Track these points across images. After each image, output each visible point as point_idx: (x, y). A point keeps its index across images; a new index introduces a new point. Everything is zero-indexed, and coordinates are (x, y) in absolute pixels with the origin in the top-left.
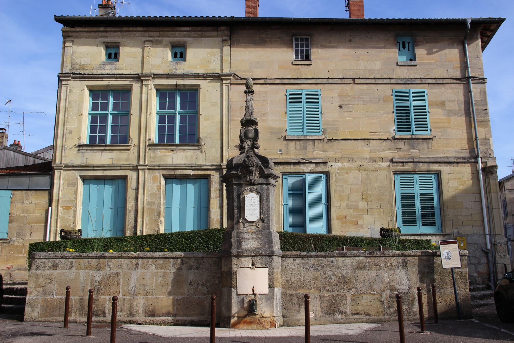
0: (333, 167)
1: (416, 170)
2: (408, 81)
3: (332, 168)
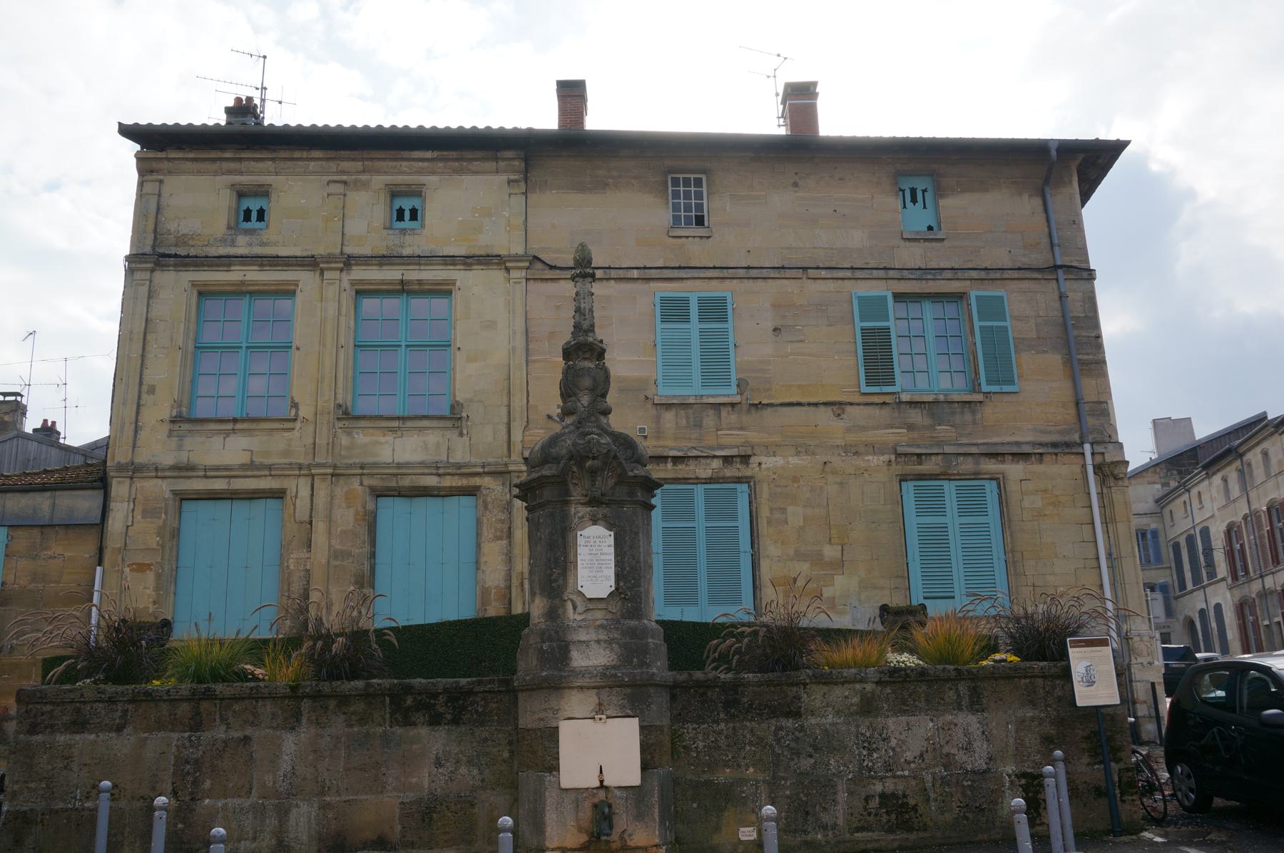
0: (763, 466)
1: (950, 472)
2: (926, 274)
3: (760, 469)
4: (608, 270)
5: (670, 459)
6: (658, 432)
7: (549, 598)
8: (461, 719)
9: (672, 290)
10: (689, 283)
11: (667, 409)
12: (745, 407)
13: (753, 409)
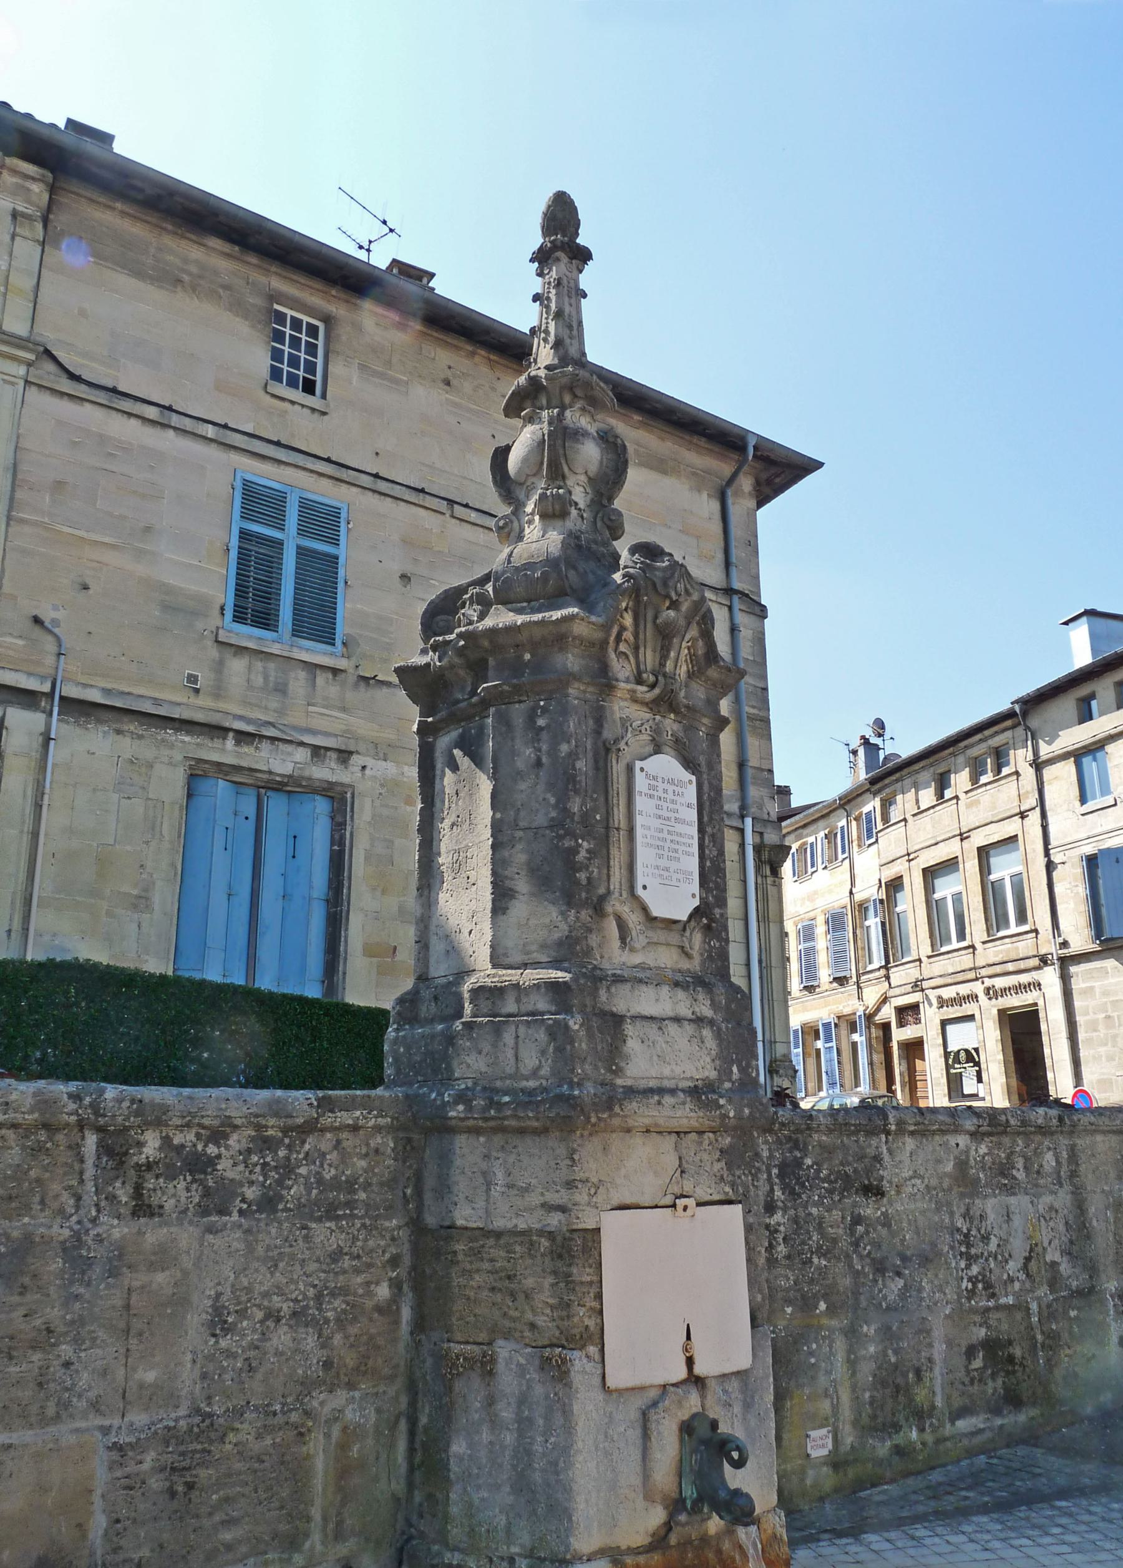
0: (367, 772)
3: (363, 775)
4: (166, 412)
5: (231, 735)
6: (219, 688)
7: (569, 904)
8: (281, 1198)
9: (266, 475)
10: (289, 471)
11: (235, 654)
12: (352, 679)
13: (362, 684)
